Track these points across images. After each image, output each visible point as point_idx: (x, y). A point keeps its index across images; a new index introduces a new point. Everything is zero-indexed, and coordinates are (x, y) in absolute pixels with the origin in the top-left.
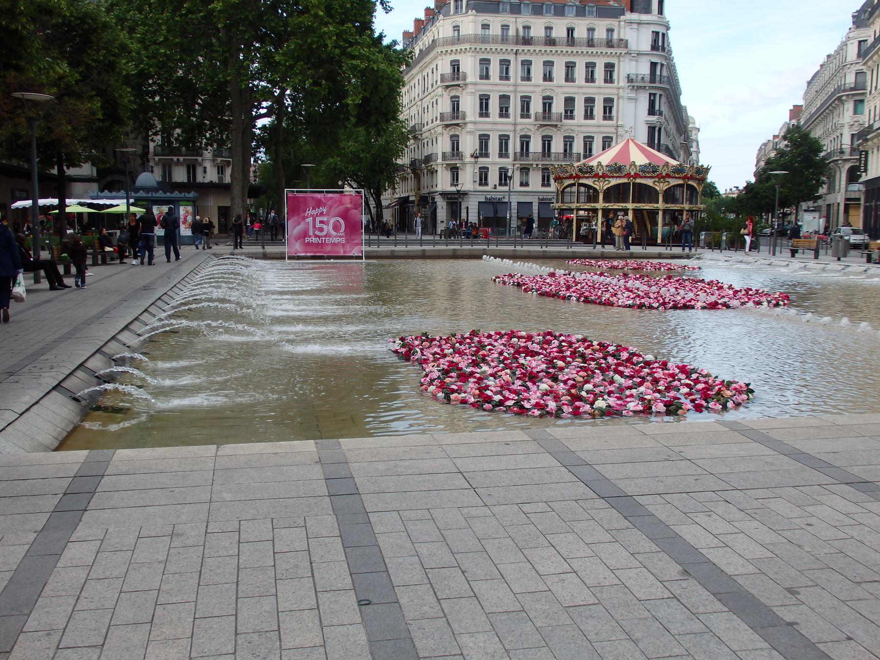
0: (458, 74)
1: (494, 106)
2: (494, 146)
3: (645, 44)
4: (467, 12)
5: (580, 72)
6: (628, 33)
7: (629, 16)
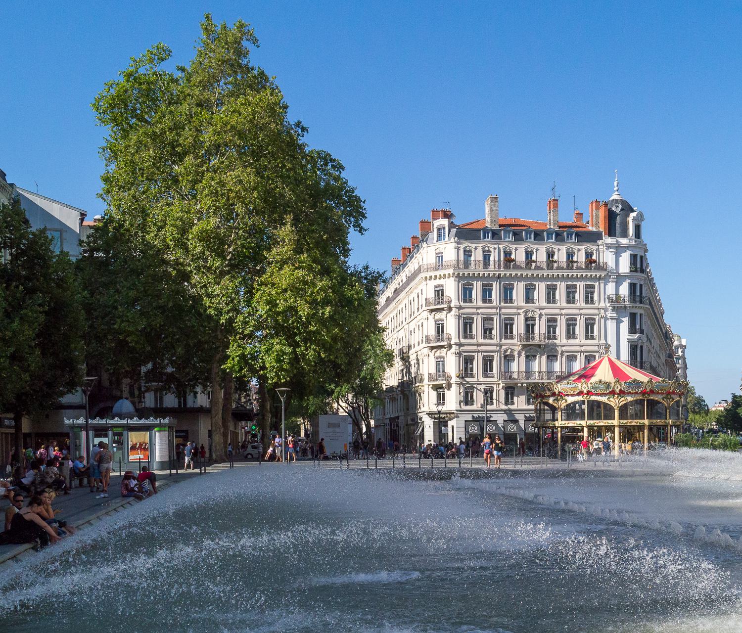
0: (442, 298)
1: (477, 328)
3: (625, 266)
6: (608, 258)
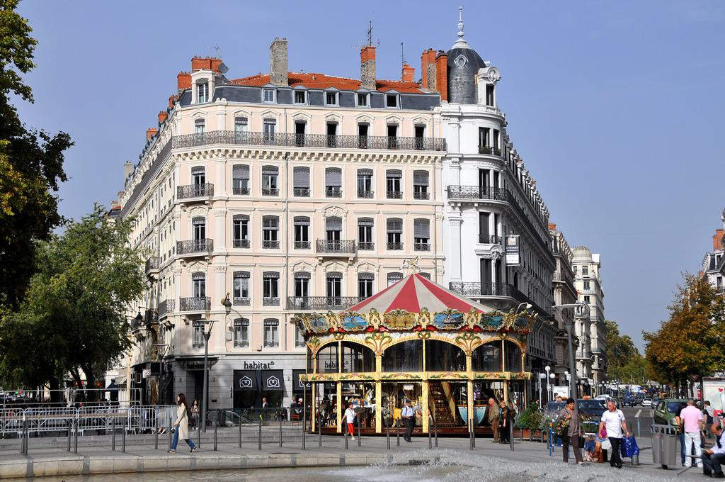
0: (203, 187)
1: (255, 232)
2: (255, 287)
3: (470, 144)
4: (214, 100)
5: (379, 184)
7: (445, 107)
